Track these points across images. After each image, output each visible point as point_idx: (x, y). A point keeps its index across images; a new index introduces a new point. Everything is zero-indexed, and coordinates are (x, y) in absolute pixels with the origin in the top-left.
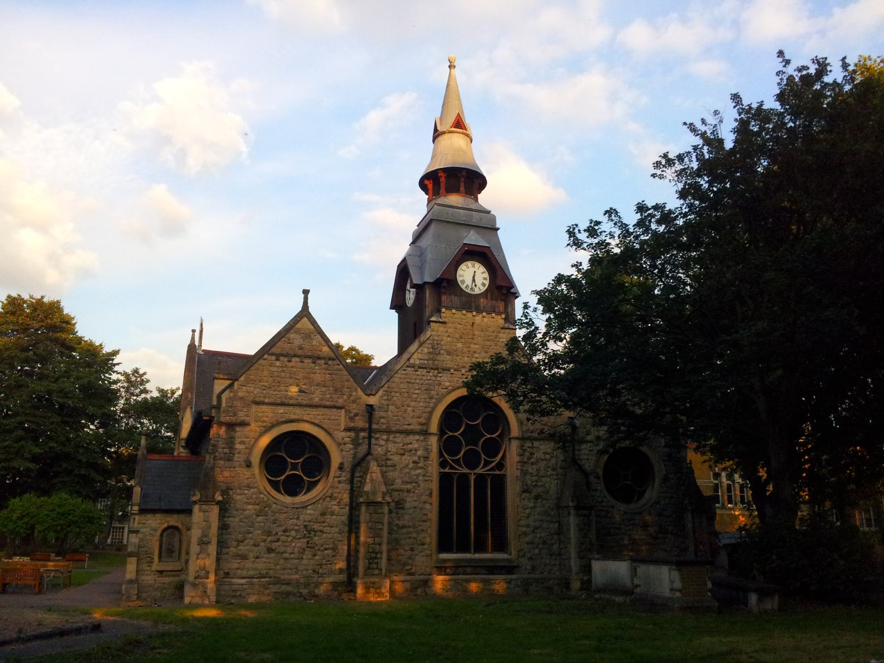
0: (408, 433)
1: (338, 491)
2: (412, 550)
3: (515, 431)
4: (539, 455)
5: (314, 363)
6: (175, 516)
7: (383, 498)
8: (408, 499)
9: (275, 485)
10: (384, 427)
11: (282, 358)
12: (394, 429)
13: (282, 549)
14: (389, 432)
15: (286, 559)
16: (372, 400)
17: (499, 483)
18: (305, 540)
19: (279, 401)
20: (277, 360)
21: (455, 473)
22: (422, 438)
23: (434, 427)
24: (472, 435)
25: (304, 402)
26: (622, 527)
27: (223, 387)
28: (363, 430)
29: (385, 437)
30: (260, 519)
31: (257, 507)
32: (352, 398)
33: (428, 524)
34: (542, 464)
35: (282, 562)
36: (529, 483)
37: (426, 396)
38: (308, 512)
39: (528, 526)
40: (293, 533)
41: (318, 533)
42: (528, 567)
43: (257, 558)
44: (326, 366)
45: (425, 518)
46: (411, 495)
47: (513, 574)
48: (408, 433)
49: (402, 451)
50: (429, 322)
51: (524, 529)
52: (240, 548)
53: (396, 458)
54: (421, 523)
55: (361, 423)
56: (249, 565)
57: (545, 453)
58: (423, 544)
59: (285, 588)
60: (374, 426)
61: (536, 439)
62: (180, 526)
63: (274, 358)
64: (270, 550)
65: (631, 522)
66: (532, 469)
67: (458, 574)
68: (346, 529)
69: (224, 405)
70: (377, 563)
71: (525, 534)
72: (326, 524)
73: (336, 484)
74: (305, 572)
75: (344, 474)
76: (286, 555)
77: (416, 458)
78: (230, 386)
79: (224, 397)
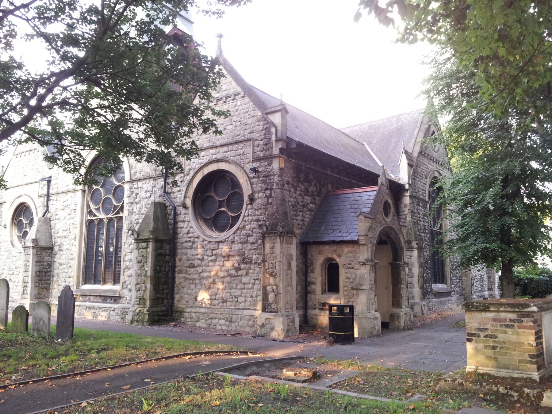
0: (66, 192)
8: (65, 243)
21: (97, 219)
33: (73, 261)
36: (134, 220)
45: (71, 257)
46: (66, 239)
47: (118, 303)
48: (66, 192)
51: (128, 264)
54: (70, 261)
57: (146, 192)
65: (214, 252)
67: (86, 301)
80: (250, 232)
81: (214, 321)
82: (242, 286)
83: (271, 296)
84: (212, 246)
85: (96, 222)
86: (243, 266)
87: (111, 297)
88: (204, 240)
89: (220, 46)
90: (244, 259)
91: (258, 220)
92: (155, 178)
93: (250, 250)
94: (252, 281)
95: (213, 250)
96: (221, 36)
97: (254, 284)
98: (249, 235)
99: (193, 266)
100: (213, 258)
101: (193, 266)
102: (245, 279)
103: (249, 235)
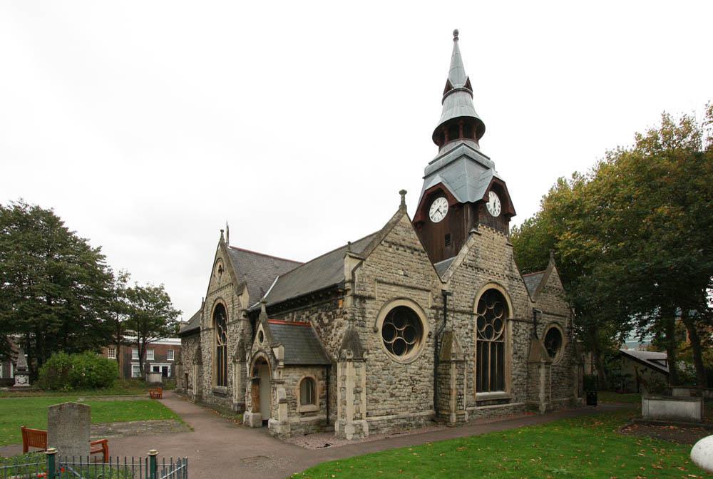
0: (463, 313)
1: (428, 352)
3: (511, 316)
4: (521, 331)
5: (412, 253)
6: (310, 369)
7: (464, 357)
9: (387, 345)
10: (452, 307)
11: (393, 246)
12: (456, 309)
13: (398, 394)
14: (455, 312)
15: (400, 401)
16: (446, 287)
17: (501, 346)
18: (411, 387)
19: (392, 281)
20: (390, 247)
22: (470, 317)
23: (475, 312)
24: (490, 315)
25: (407, 285)
27: (355, 265)
28: (440, 309)
29: (452, 315)
30: (385, 372)
31: (383, 364)
32: (434, 284)
34: (522, 337)
35: (399, 402)
37: (472, 287)
38: (413, 367)
39: (515, 374)
40: (404, 382)
41: (418, 382)
43: (385, 401)
44: (419, 257)
48: (463, 313)
49: (461, 325)
50: (470, 234)
51: (513, 376)
52: (375, 394)
53: (457, 330)
55: (439, 304)
56: (380, 407)
58: (470, 388)
59: (402, 421)
60: (447, 307)
62: (314, 377)
63: (387, 245)
64: (392, 395)
66: (518, 340)
68: (433, 379)
69: (356, 280)
70: (461, 402)
71: (514, 379)
72: (422, 376)
73: (427, 348)
74: (412, 409)
75: (431, 340)
76: (401, 398)
77: (467, 331)
78: (360, 264)
79: (357, 273)
92: (528, 323)
96: (403, 193)
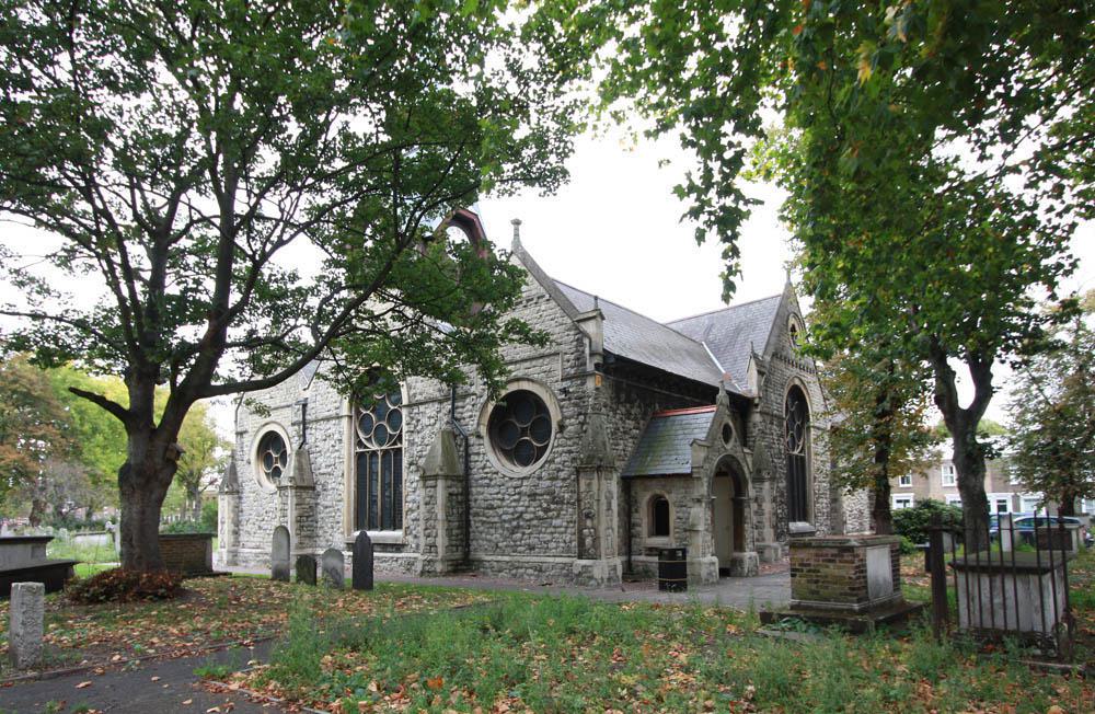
0: (328, 419)
2: (332, 528)
13: (266, 527)
14: (317, 421)
26: (507, 497)
42: (414, 546)
45: (339, 498)
47: (401, 552)
48: (328, 419)
51: (410, 505)
57: (429, 418)
60: (308, 417)
61: (422, 404)
64: (260, 528)
65: (517, 490)
77: (333, 443)
80: (560, 466)
81: (522, 571)
82: (553, 530)
83: (588, 541)
84: (515, 483)
85: (368, 455)
86: (552, 506)
87: (392, 545)
88: (504, 476)
89: (517, 235)
90: (555, 498)
91: (570, 452)
92: (440, 402)
93: (561, 487)
94: (565, 524)
95: (515, 488)
97: (567, 527)
98: (559, 470)
99: (491, 507)
100: (516, 497)
101: (491, 507)
102: (556, 522)
103: (559, 470)
